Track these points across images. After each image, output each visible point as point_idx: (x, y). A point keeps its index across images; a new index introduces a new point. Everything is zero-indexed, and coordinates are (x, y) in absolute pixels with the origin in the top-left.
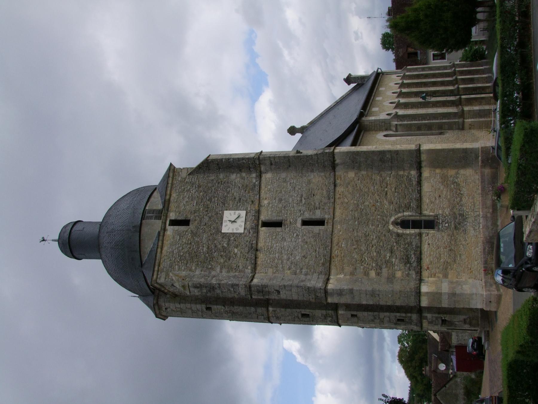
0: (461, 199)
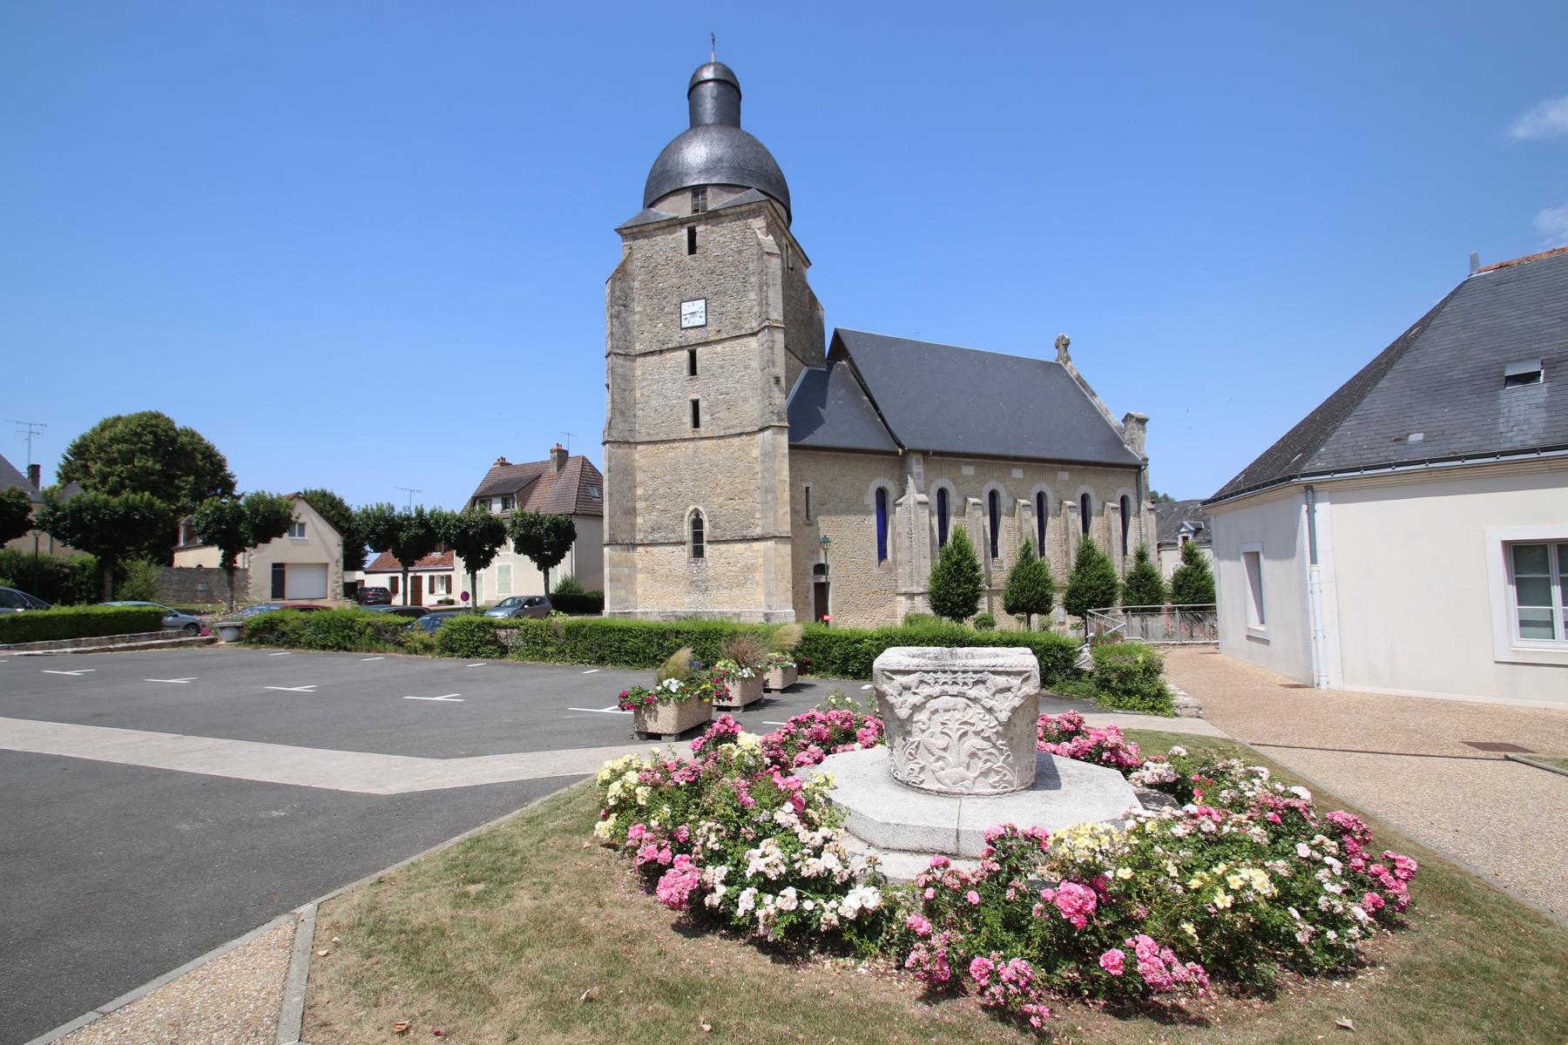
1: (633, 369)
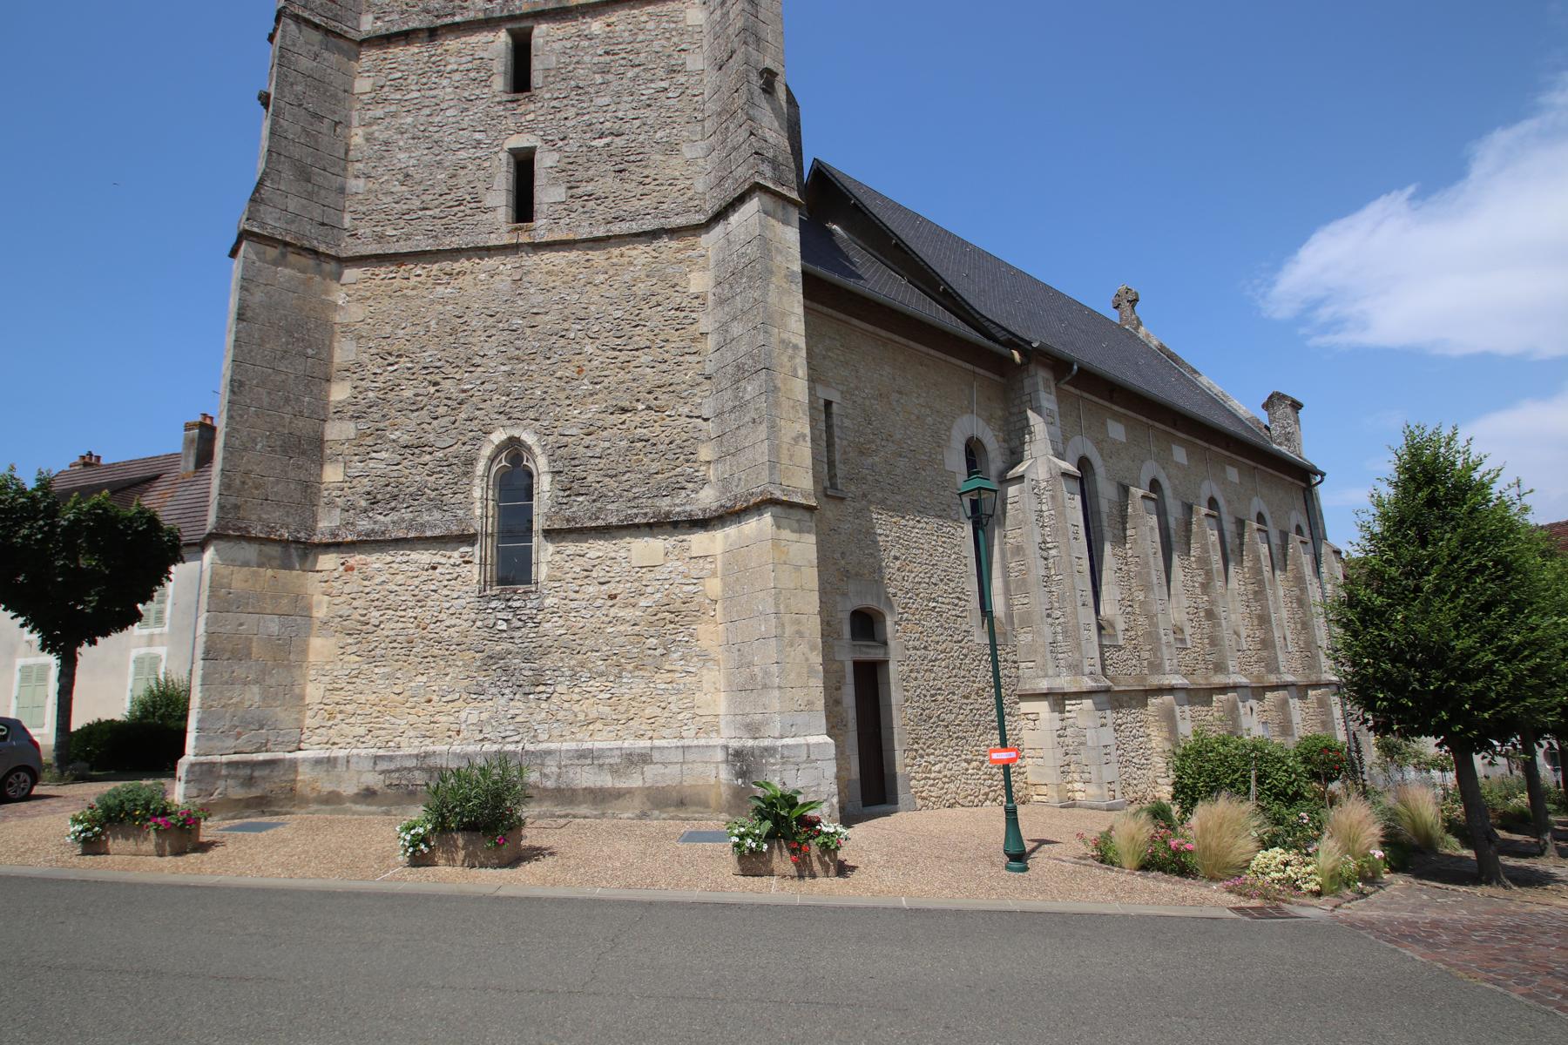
0: (601, 675)
1: (350, 77)
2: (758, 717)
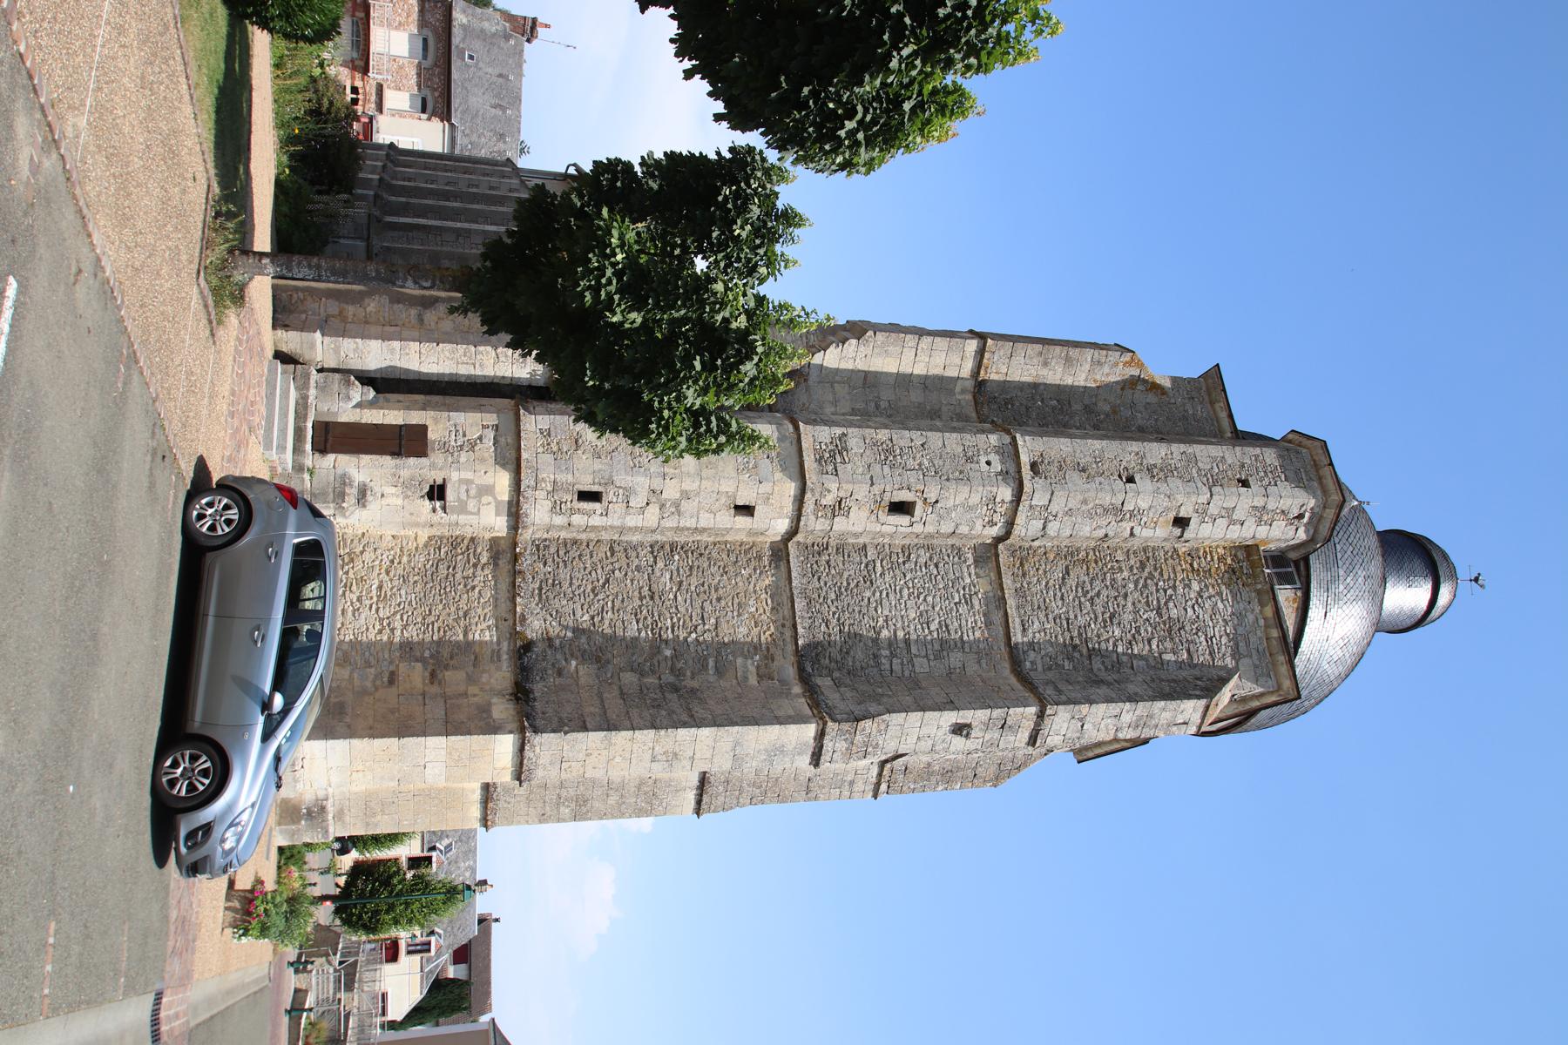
2: (347, 819)
